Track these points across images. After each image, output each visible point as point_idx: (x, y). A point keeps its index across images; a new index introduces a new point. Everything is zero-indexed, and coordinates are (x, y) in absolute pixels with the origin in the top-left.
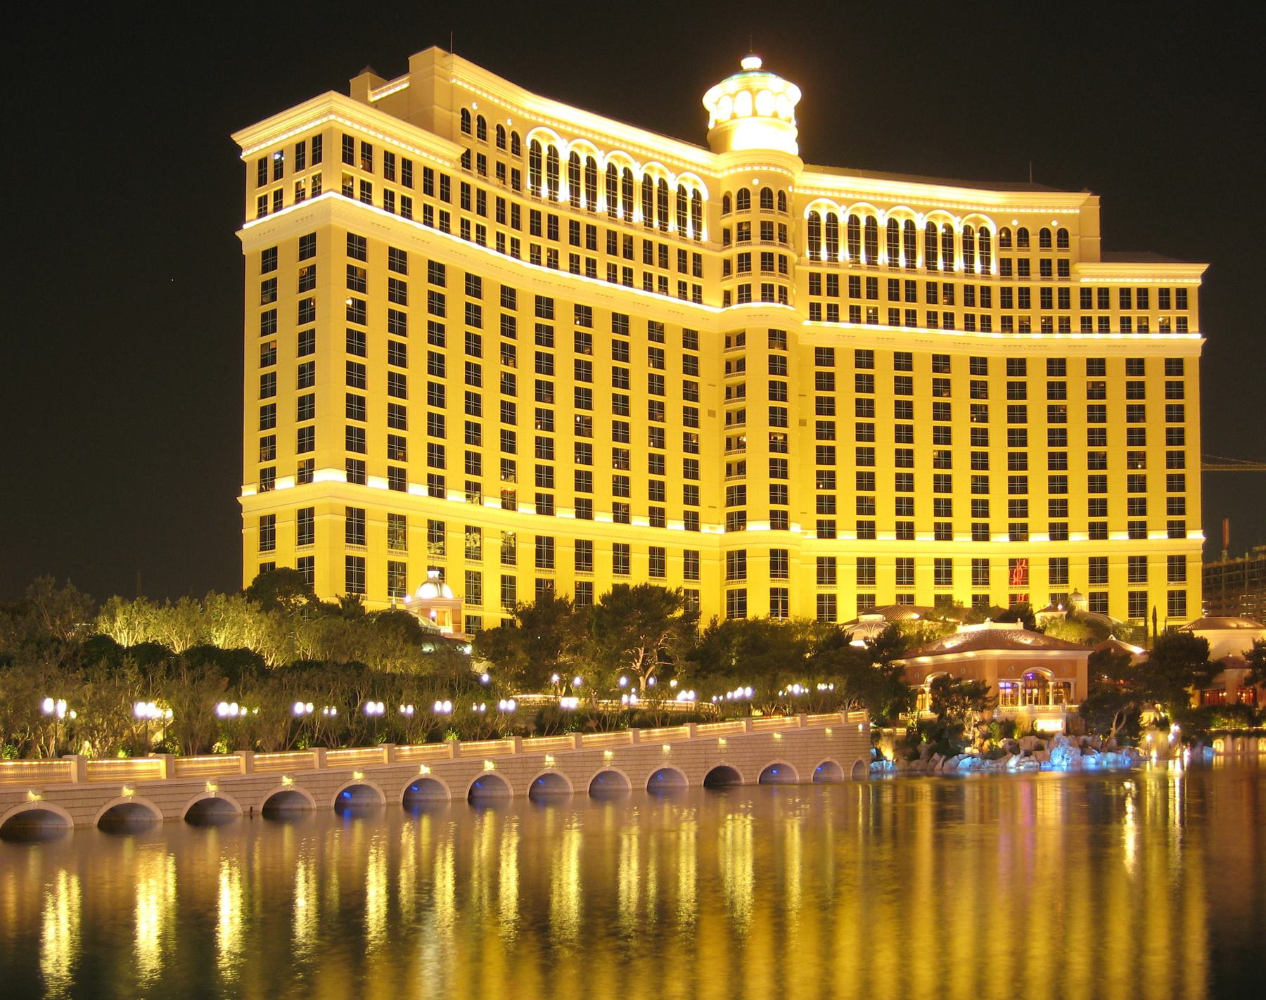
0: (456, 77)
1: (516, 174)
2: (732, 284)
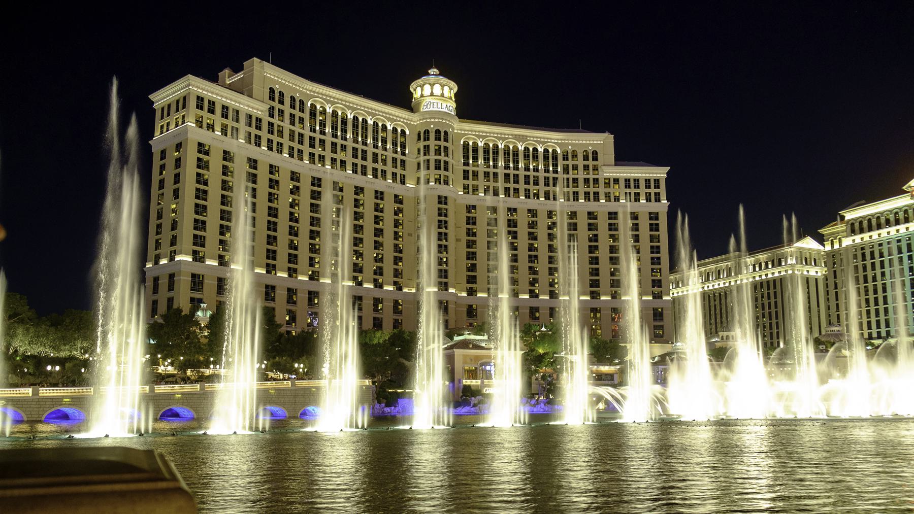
0: (267, 73)
1: (302, 120)
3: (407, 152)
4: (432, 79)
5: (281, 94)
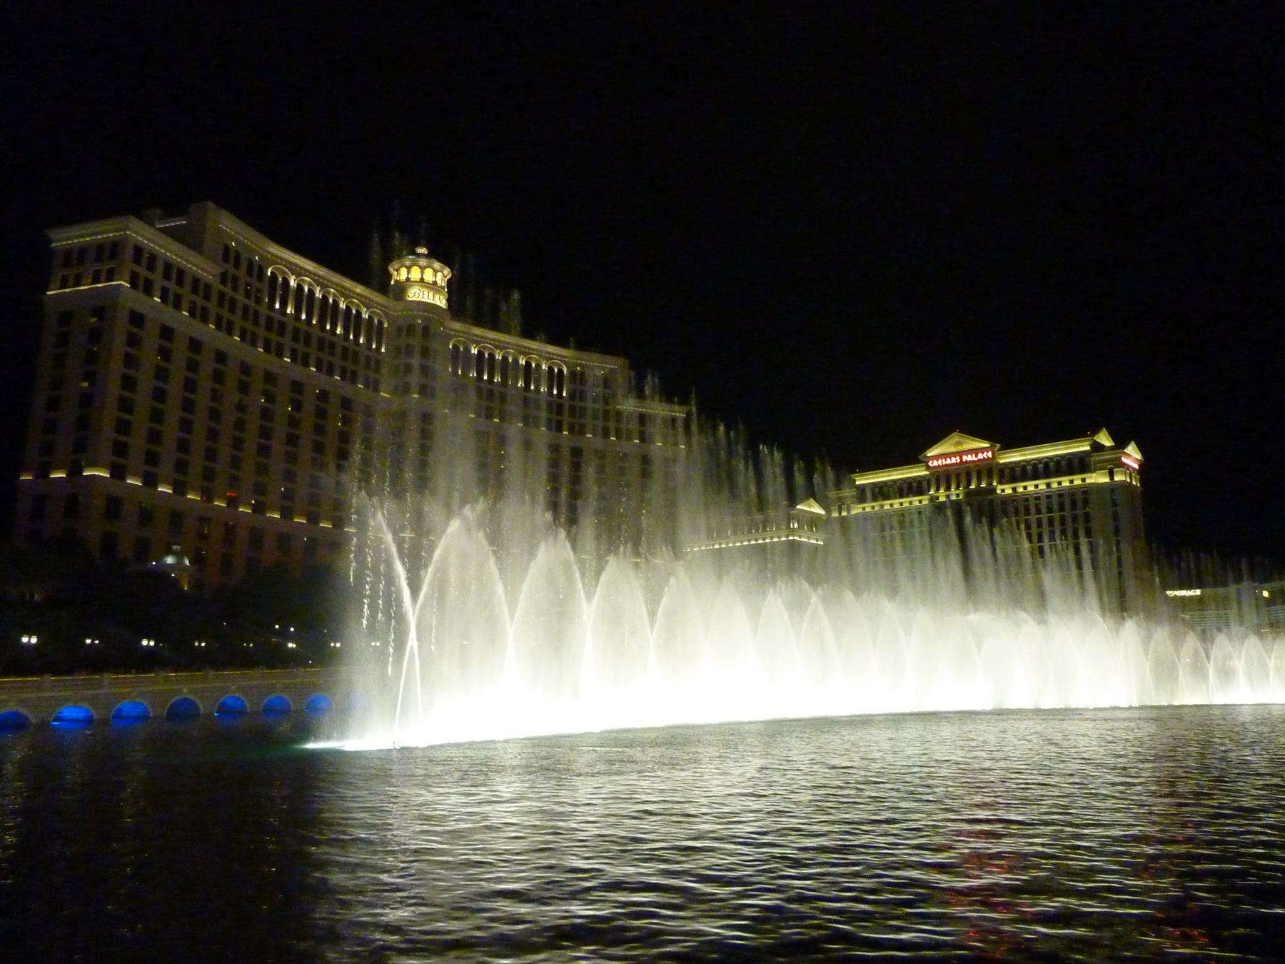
3: (383, 350)
4: (423, 262)
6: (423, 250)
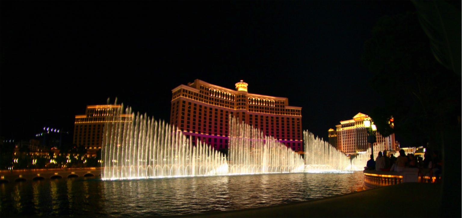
2: (238, 107)
4: (241, 83)
5: (203, 87)
6: (242, 81)
